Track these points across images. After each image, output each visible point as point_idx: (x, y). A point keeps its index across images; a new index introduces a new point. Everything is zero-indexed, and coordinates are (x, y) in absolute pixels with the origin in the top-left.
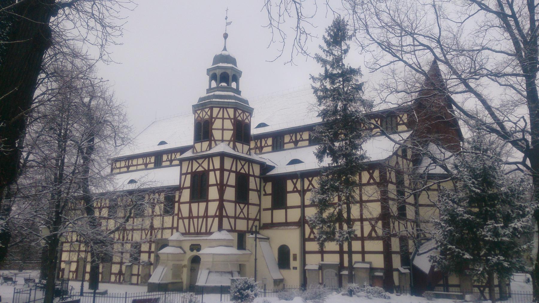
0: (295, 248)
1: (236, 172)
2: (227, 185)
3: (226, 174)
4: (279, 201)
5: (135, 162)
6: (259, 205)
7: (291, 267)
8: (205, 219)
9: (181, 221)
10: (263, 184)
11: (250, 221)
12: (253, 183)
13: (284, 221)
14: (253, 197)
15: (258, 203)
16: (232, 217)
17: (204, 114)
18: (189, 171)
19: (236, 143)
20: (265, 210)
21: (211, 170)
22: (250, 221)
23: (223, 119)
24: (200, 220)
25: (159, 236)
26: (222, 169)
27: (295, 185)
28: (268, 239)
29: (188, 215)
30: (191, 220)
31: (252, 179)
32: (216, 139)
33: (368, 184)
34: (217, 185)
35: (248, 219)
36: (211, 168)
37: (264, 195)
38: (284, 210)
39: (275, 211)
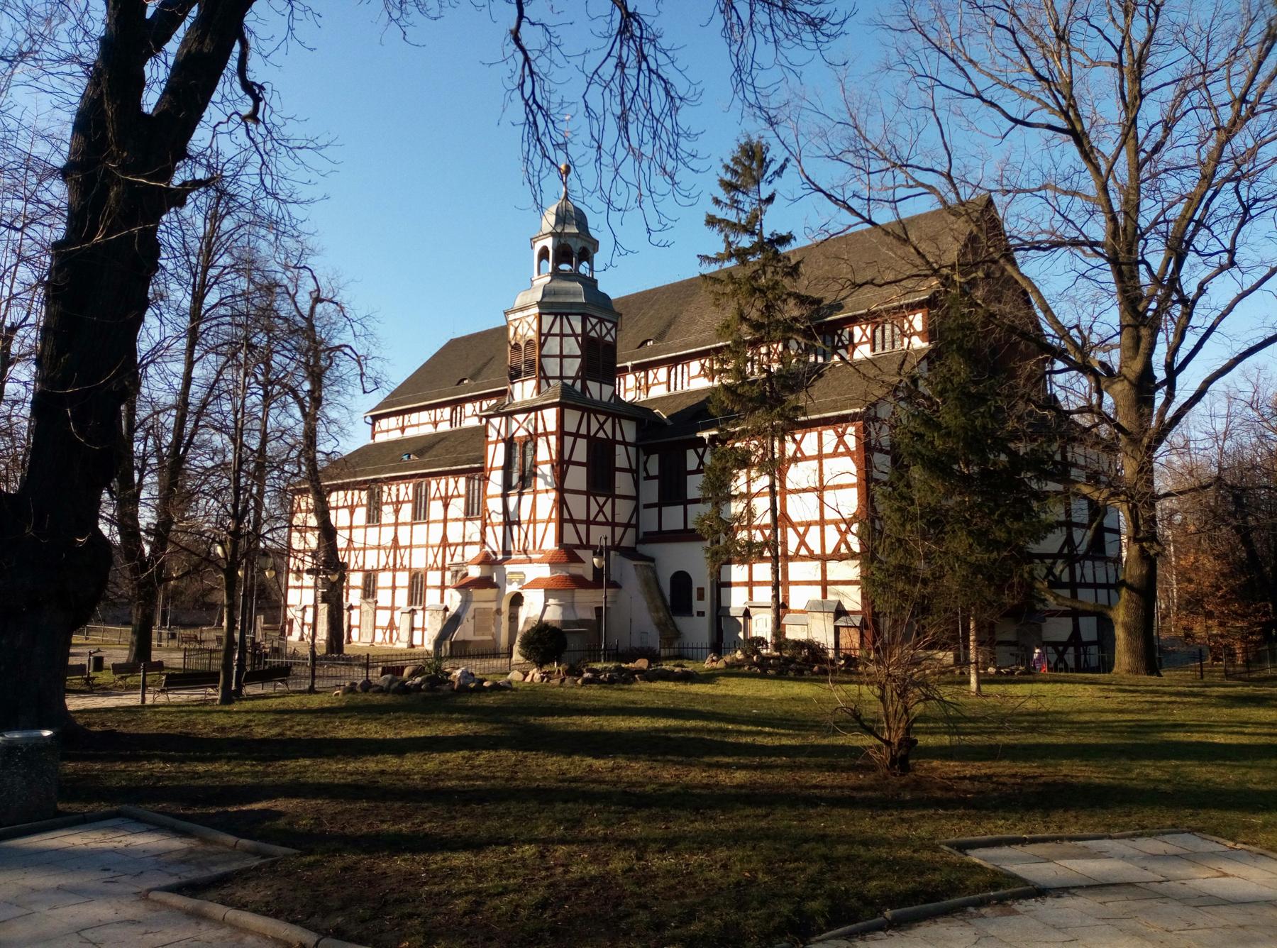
0: (701, 578)
1: (587, 437)
2: (570, 462)
3: (568, 441)
4: (673, 493)
5: (415, 417)
6: (636, 498)
7: (695, 612)
9: (489, 529)
10: (643, 458)
11: (617, 529)
12: (621, 457)
13: (681, 527)
14: (623, 483)
15: (634, 494)
16: (581, 522)
17: (526, 326)
19: (589, 383)
20: (647, 506)
21: (541, 435)
22: (617, 529)
23: (562, 335)
25: (457, 559)
26: (561, 433)
27: (701, 458)
28: (652, 560)
31: (620, 449)
32: (549, 374)
33: (835, 454)
35: (613, 524)
36: (540, 430)
37: (646, 479)
39: (665, 509)
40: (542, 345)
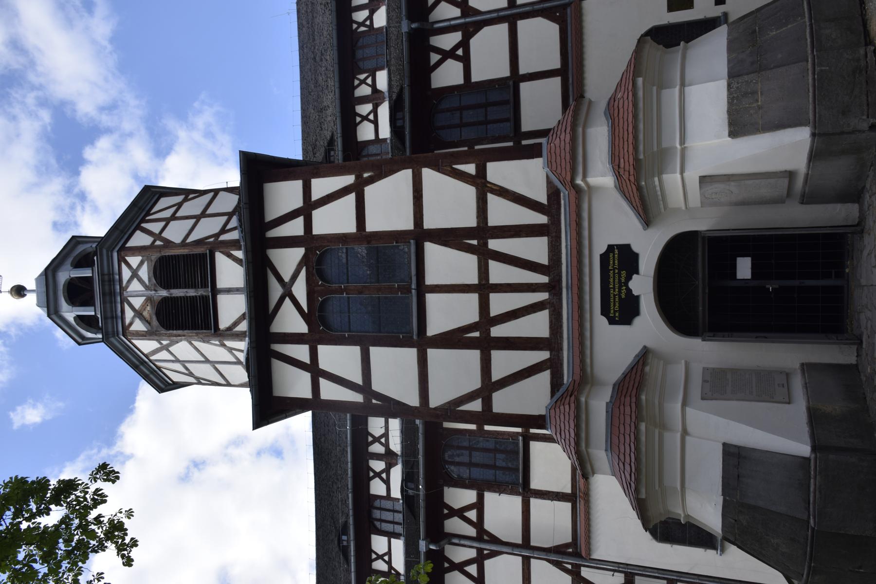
8: (494, 244)
13: (557, 81)
18: (301, 352)
24: (499, 273)
27: (447, 55)
29: (474, 355)
30: (497, 331)
34: (358, 189)
36: (295, 228)
38: (524, 87)
40: (168, 243)
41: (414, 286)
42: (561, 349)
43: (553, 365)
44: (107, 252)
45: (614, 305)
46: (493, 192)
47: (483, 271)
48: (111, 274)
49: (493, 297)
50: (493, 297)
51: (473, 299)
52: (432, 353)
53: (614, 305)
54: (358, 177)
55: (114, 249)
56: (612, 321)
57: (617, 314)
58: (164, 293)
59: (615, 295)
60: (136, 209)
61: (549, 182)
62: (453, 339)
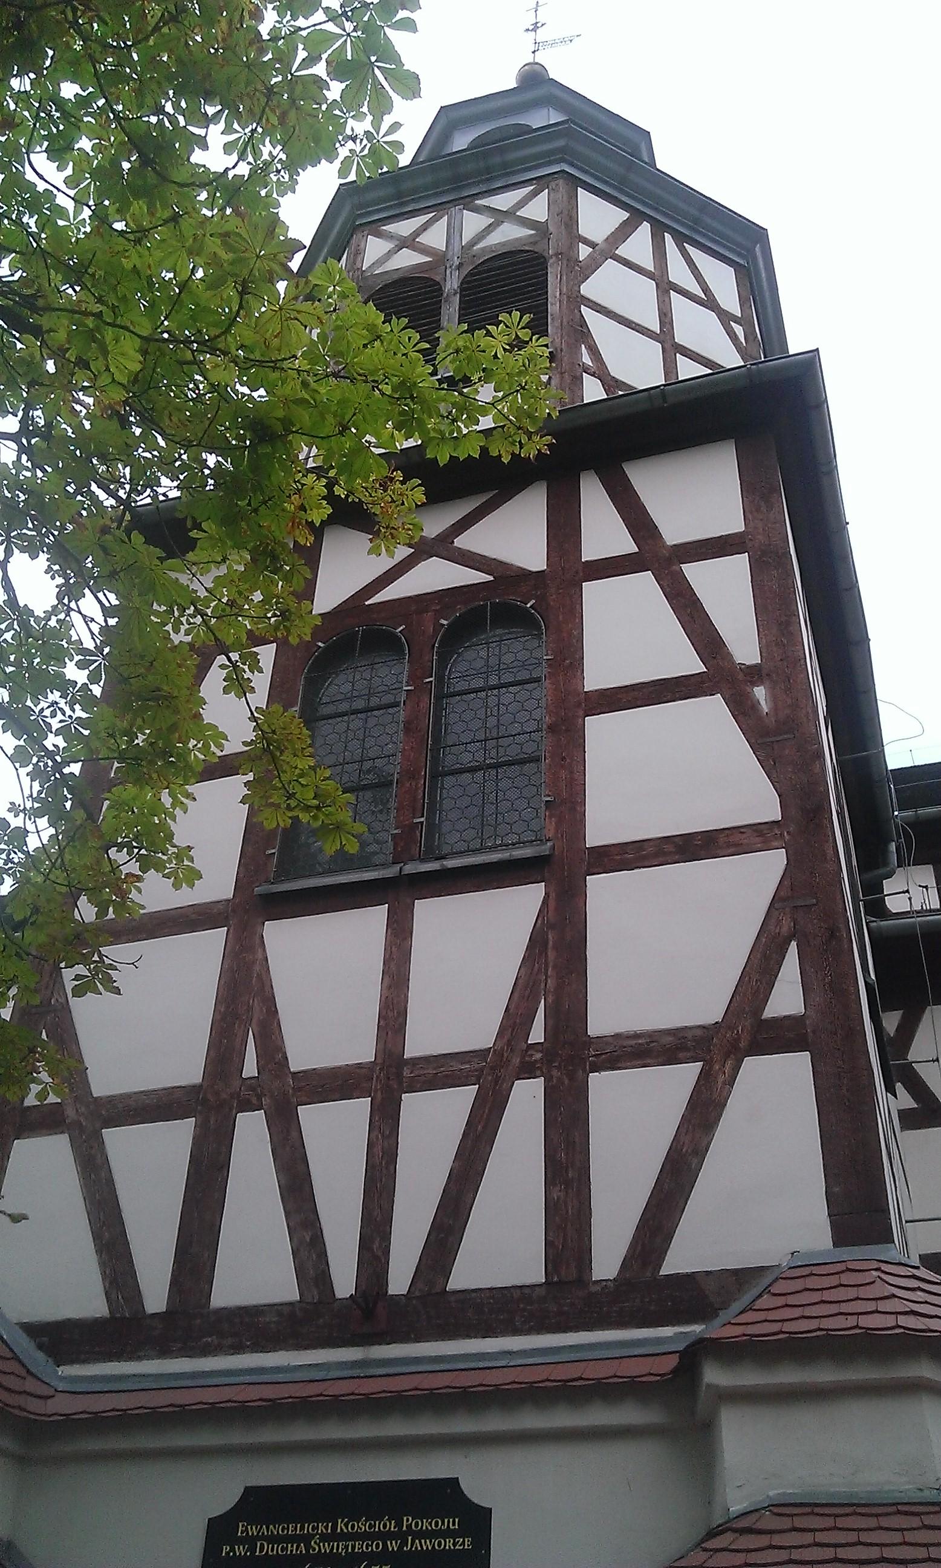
8: (527, 1099)
24: (433, 1122)
30: (251, 1130)
34: (718, 675)
37: (910, 1120)
41: (410, 868)
42: (165, 1352)
43: (123, 1329)
44: (562, 150)
45: (272, 1539)
46: (705, 1078)
47: (440, 1072)
48: (507, 169)
49: (357, 1110)
50: (357, 1110)
51: (361, 1049)
52: (212, 943)
53: (272, 1539)
54: (754, 674)
55: (572, 165)
56: (219, 1530)
57: (240, 1550)
58: (452, 283)
59: (306, 1539)
60: (695, 212)
61: (742, 1277)
62: (245, 1000)
